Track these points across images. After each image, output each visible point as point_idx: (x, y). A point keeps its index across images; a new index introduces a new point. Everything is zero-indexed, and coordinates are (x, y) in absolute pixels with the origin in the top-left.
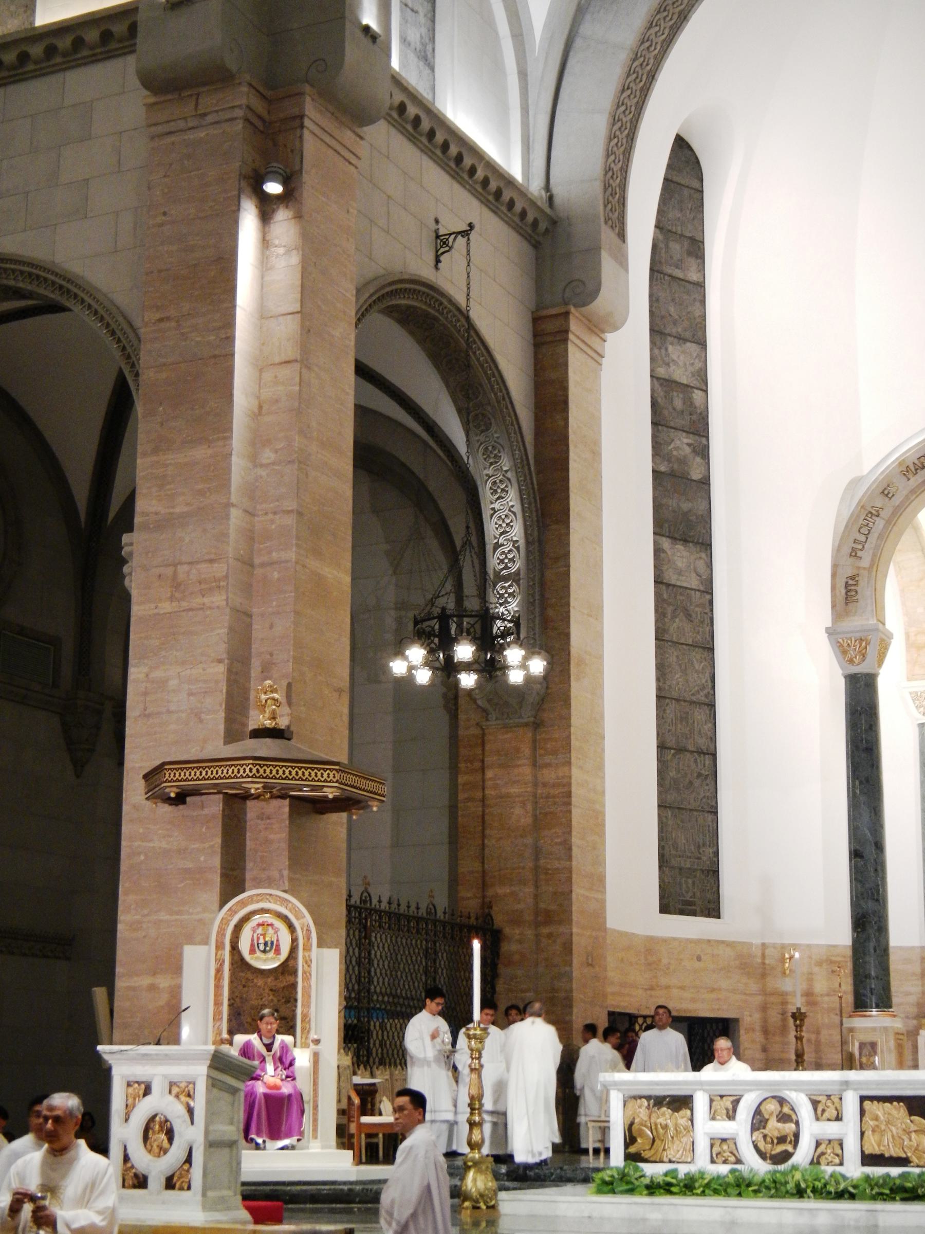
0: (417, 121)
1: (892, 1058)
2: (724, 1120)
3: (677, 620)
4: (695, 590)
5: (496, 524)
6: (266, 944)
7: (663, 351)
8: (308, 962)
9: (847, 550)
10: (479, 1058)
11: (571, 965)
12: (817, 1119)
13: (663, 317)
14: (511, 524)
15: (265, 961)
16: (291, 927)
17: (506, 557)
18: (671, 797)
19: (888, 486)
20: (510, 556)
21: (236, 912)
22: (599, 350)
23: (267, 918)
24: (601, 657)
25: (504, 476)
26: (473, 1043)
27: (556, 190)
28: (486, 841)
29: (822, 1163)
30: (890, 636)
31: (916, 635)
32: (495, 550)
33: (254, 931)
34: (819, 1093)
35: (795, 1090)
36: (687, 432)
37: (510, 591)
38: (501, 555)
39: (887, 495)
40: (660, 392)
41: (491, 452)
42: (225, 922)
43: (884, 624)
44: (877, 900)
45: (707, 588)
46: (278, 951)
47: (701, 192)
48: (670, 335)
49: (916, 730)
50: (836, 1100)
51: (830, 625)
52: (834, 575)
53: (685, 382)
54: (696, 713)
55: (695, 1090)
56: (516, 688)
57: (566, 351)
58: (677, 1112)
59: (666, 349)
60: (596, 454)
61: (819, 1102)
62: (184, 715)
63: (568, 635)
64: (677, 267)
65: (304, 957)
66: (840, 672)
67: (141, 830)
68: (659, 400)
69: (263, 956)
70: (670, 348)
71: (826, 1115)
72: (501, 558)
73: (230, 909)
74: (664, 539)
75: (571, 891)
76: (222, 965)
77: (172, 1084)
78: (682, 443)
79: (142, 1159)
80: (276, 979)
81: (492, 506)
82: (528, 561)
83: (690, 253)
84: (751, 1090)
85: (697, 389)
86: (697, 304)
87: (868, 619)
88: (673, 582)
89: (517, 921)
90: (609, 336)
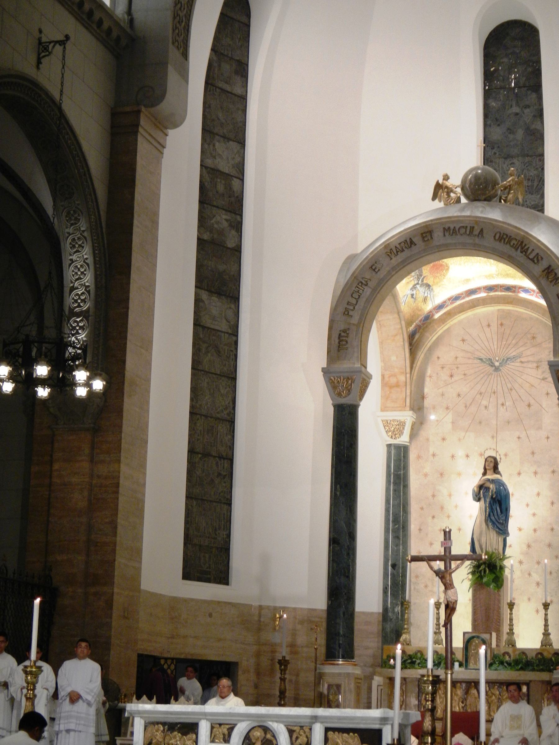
1: (352, 697)
2: (221, 743)
3: (209, 354)
4: (224, 332)
5: (73, 271)
7: (211, 147)
9: (341, 309)
10: (34, 689)
11: (111, 618)
13: (213, 120)
14: (85, 273)
17: (79, 298)
19: (376, 263)
20: (82, 298)
22: (161, 141)
24: (148, 380)
25: (81, 234)
26: (29, 678)
27: (138, 15)
28: (50, 519)
30: (370, 377)
31: (389, 377)
32: (71, 291)
34: (295, 724)
35: (277, 722)
36: (226, 210)
37: (81, 324)
38: (75, 296)
39: (374, 270)
40: (207, 178)
41: (73, 215)
43: (366, 368)
44: (348, 577)
47: (248, 26)
48: (218, 135)
49: (384, 450)
50: (307, 730)
51: (326, 366)
52: (330, 328)
53: (227, 172)
54: (220, 427)
55: (201, 719)
56: (81, 400)
57: (136, 140)
58: (186, 735)
59: (214, 145)
60: (155, 223)
61: (294, 731)
63: (124, 362)
64: (227, 83)
66: (331, 402)
68: (206, 184)
70: (217, 144)
72: (75, 298)
74: (203, 291)
75: (115, 560)
81: (71, 257)
82: (97, 303)
83: (237, 72)
84: (243, 721)
85: (235, 177)
86: (240, 112)
87: (354, 364)
88: (208, 325)
90: (171, 132)
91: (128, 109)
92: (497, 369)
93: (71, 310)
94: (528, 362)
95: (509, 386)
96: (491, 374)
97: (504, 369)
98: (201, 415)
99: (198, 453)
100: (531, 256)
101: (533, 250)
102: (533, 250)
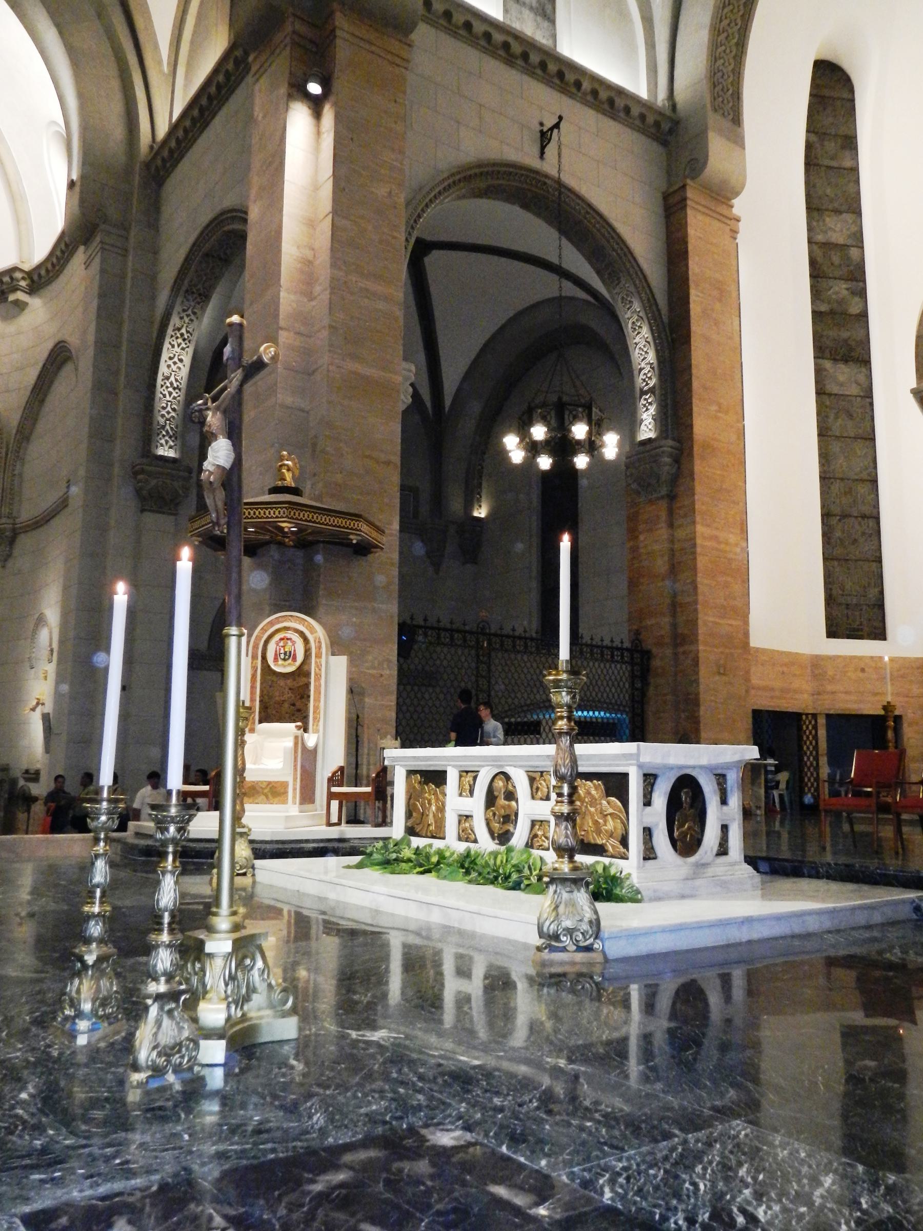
0: (506, 46)
4: (856, 396)
6: (285, 653)
7: (821, 223)
8: (319, 666)
12: (533, 798)
13: (820, 198)
15: (284, 666)
16: (306, 640)
18: (838, 551)
20: (649, 375)
21: (266, 631)
23: (289, 634)
33: (277, 645)
40: (819, 253)
45: (868, 394)
46: (294, 659)
59: (824, 221)
64: (832, 159)
65: (316, 662)
68: (818, 259)
70: (828, 219)
73: (262, 629)
74: (826, 361)
76: (256, 671)
78: (840, 289)
82: (662, 376)
83: (843, 147)
89: (660, 644)
90: (735, 202)
91: (676, 187)
93: (641, 390)
98: (835, 479)
99: (835, 515)
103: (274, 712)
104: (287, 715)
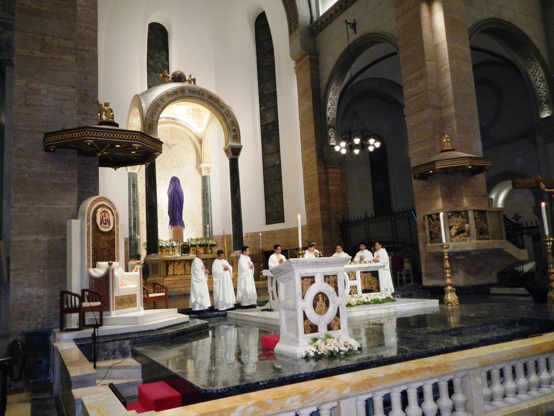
6: (106, 220)
8: (118, 229)
12: (350, 280)
21: (93, 205)
29: (352, 293)
39: (162, 101)
42: (90, 209)
46: (109, 224)
62: (52, 109)
67: (25, 162)
69: (104, 225)
71: (352, 278)
73: (91, 204)
77: (325, 277)
79: (313, 317)
80: (109, 236)
92: (170, 148)
94: (181, 146)
95: (175, 154)
96: (167, 149)
97: (173, 148)
100: (221, 106)
101: (221, 104)
102: (221, 104)
103: (100, 255)
104: (106, 257)
